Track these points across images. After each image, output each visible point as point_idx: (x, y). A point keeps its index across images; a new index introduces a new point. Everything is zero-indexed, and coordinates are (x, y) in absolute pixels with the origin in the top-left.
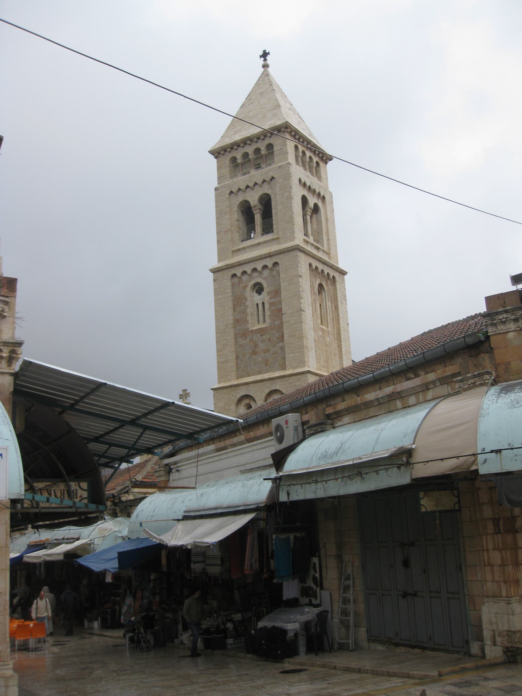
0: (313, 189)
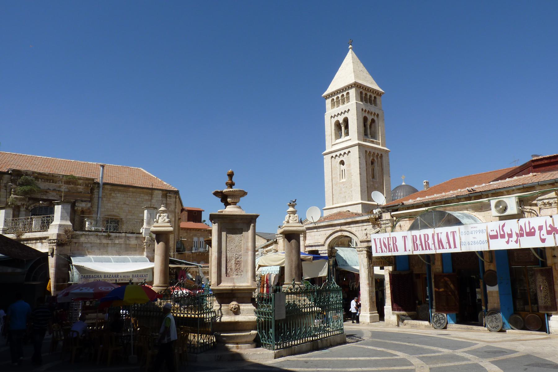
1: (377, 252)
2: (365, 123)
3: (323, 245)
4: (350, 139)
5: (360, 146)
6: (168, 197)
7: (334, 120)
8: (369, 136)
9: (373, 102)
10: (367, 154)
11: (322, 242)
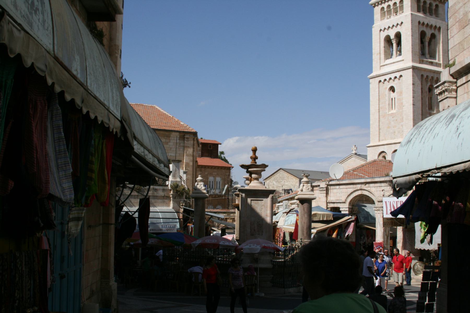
0: (431, 24)
1: (387, 214)
2: (423, 40)
3: (344, 203)
4: (403, 60)
5: (415, 70)
6: (186, 139)
7: (384, 35)
8: (427, 56)
9: (433, 12)
10: (424, 79)
11: (343, 200)
